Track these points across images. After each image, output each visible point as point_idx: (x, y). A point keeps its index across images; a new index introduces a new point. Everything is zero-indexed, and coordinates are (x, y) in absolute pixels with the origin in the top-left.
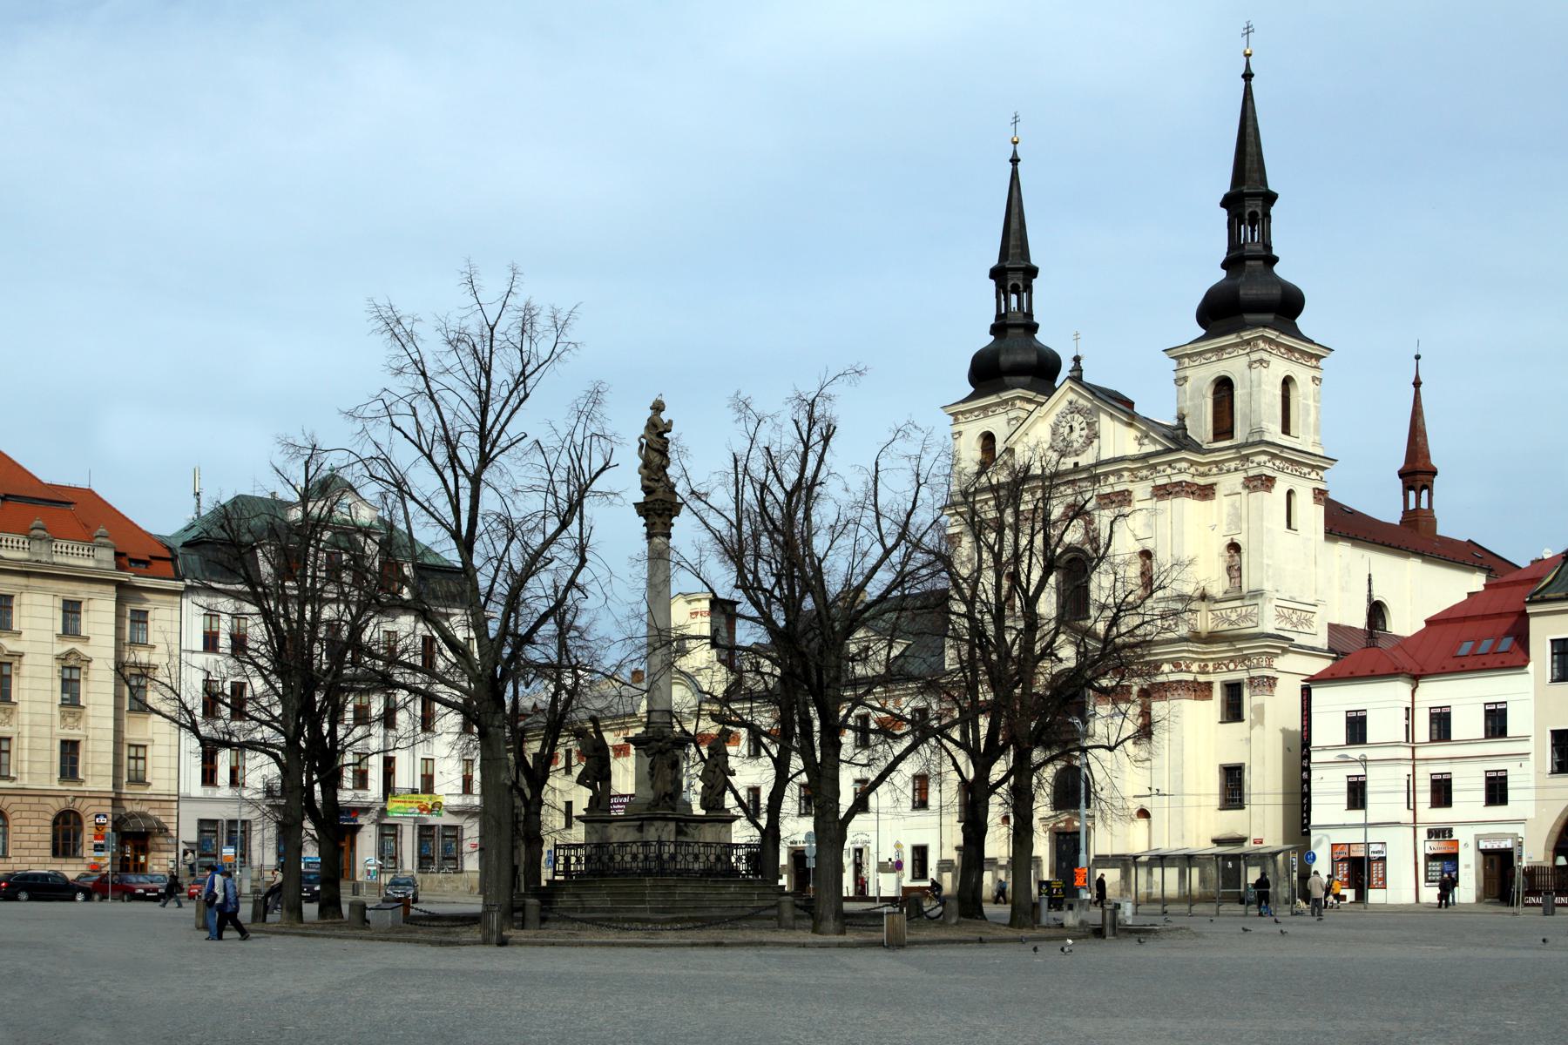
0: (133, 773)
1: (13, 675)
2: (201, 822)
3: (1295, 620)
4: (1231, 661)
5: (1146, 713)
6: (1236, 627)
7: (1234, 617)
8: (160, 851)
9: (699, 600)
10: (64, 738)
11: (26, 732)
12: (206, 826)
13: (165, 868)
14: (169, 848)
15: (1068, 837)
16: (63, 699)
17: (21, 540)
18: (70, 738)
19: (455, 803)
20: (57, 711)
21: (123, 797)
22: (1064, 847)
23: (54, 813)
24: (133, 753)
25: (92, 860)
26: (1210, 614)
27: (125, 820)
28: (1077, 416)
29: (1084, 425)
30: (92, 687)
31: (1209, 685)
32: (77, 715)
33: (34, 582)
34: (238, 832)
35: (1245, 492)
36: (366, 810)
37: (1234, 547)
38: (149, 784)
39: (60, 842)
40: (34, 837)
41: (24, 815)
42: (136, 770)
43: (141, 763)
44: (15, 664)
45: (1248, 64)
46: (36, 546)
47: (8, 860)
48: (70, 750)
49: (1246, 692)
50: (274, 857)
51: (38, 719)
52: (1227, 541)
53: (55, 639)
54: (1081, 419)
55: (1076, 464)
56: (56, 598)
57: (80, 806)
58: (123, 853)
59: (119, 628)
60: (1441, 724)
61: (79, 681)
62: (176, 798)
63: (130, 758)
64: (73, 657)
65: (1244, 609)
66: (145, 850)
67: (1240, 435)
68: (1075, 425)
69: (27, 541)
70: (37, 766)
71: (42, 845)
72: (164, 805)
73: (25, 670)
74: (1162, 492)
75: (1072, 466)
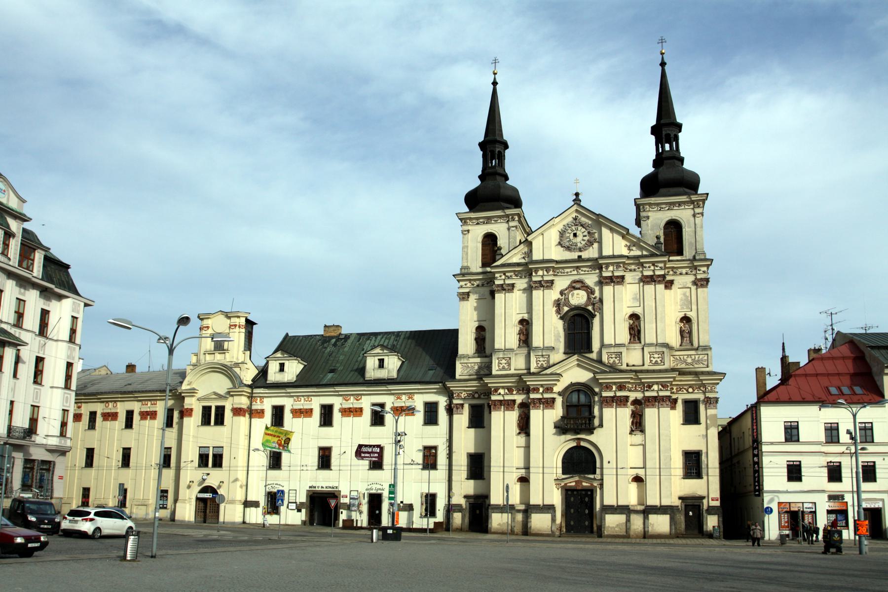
4: (690, 387)
6: (691, 366)
7: (689, 360)
9: (239, 317)
15: (575, 493)
22: (572, 499)
26: (671, 357)
28: (580, 228)
29: (586, 233)
35: (694, 288)
37: (686, 320)
45: (663, 58)
49: (702, 407)
52: (682, 315)
54: (583, 230)
55: (580, 257)
65: (697, 356)
67: (688, 253)
68: (578, 233)
74: (647, 280)
75: (576, 257)
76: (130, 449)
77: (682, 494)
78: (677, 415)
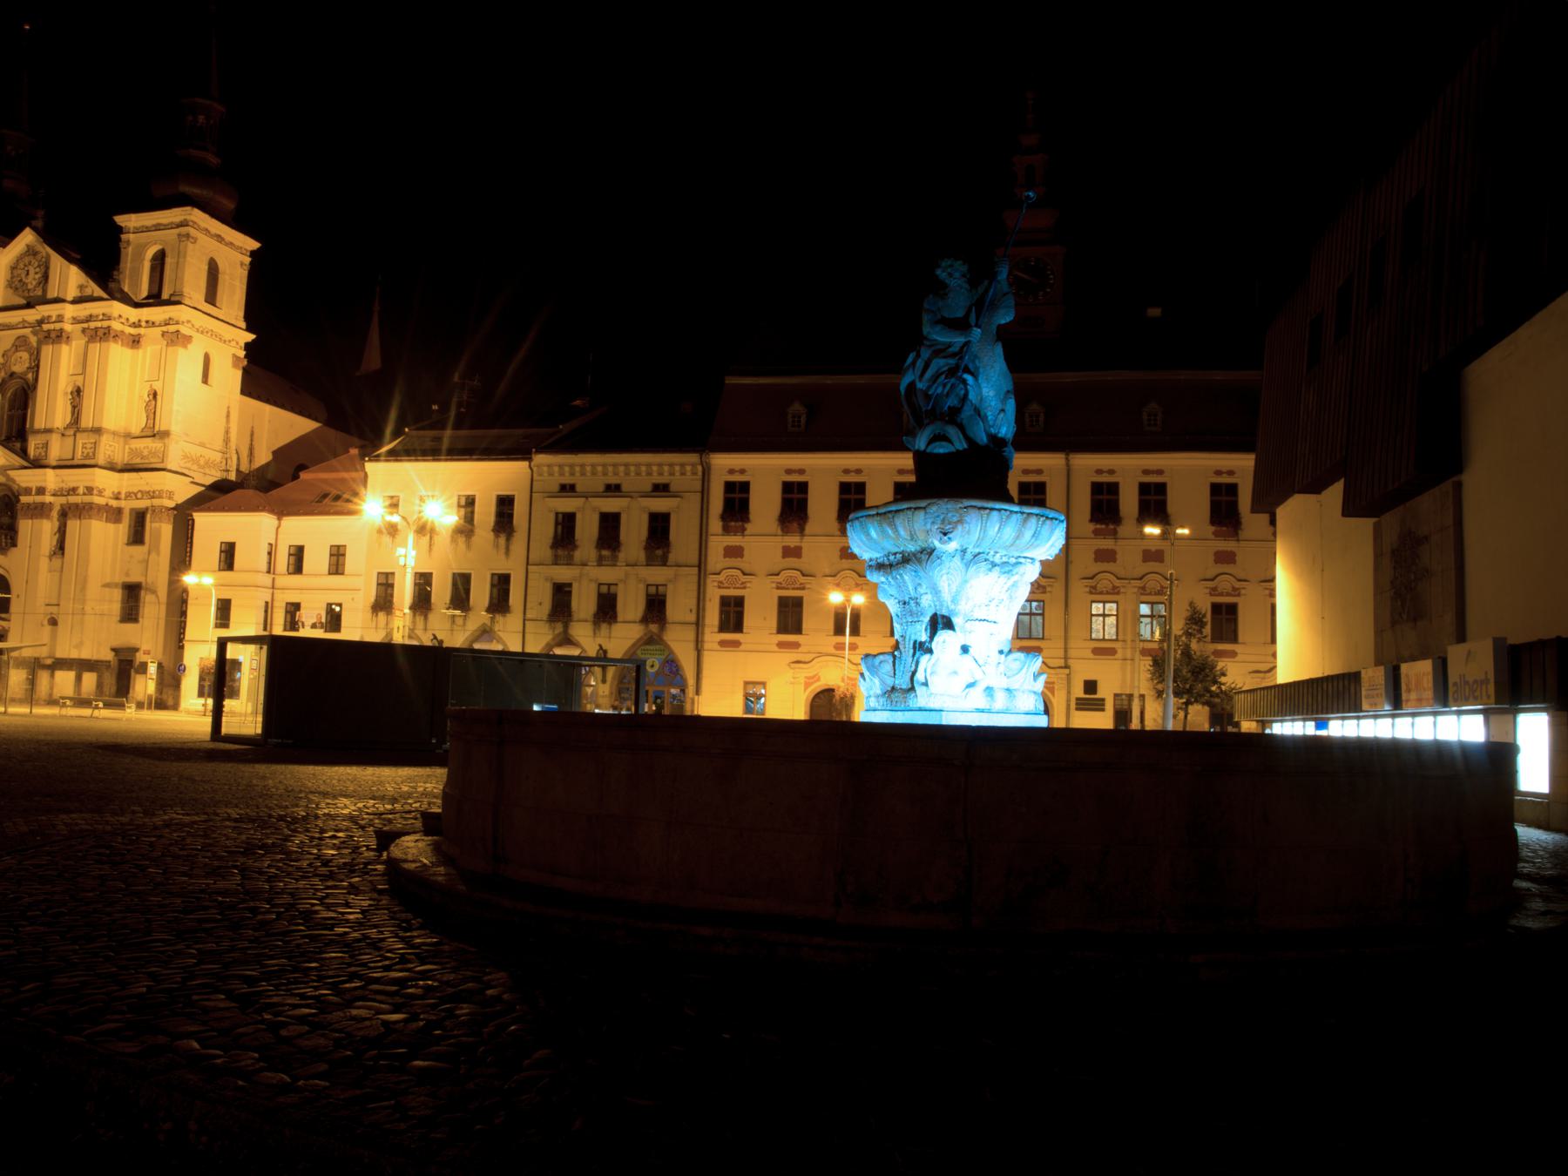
3: (202, 462)
5: (62, 532)
6: (147, 461)
31: (119, 511)
60: (297, 558)
77: (117, 643)
78: (123, 529)
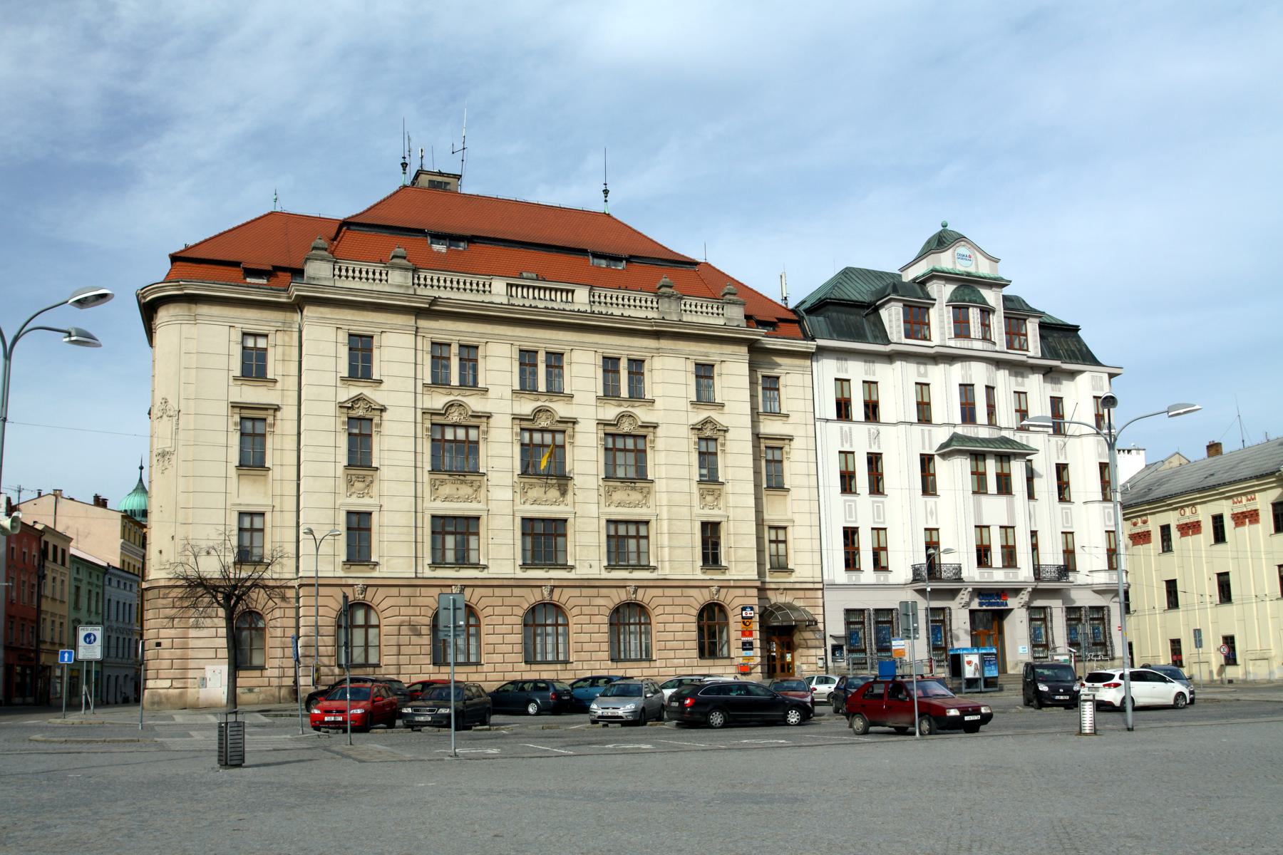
0: (774, 559)
1: (648, 450)
2: (848, 612)
8: (808, 648)
10: (705, 519)
11: (665, 515)
12: (853, 616)
13: (813, 667)
14: (817, 643)
16: (701, 475)
17: (649, 299)
18: (711, 519)
19: (1103, 581)
20: (695, 487)
21: (768, 586)
23: (698, 607)
24: (773, 538)
25: (741, 661)
27: (772, 613)
30: (730, 460)
32: (717, 493)
33: (665, 344)
34: (886, 621)
36: (1016, 592)
38: (792, 571)
39: (706, 641)
40: (679, 636)
41: (668, 609)
42: (778, 555)
43: (781, 546)
44: (650, 437)
46: (665, 305)
47: (653, 664)
48: (711, 532)
50: (925, 648)
51: (677, 498)
53: (690, 408)
56: (688, 361)
57: (727, 598)
58: (769, 651)
59: (753, 396)
61: (716, 454)
62: (820, 586)
63: (771, 541)
64: (709, 426)
66: (790, 647)
69: (655, 300)
70: (678, 552)
71: (688, 645)
72: (809, 594)
73: (660, 444)
76: (1227, 574)
